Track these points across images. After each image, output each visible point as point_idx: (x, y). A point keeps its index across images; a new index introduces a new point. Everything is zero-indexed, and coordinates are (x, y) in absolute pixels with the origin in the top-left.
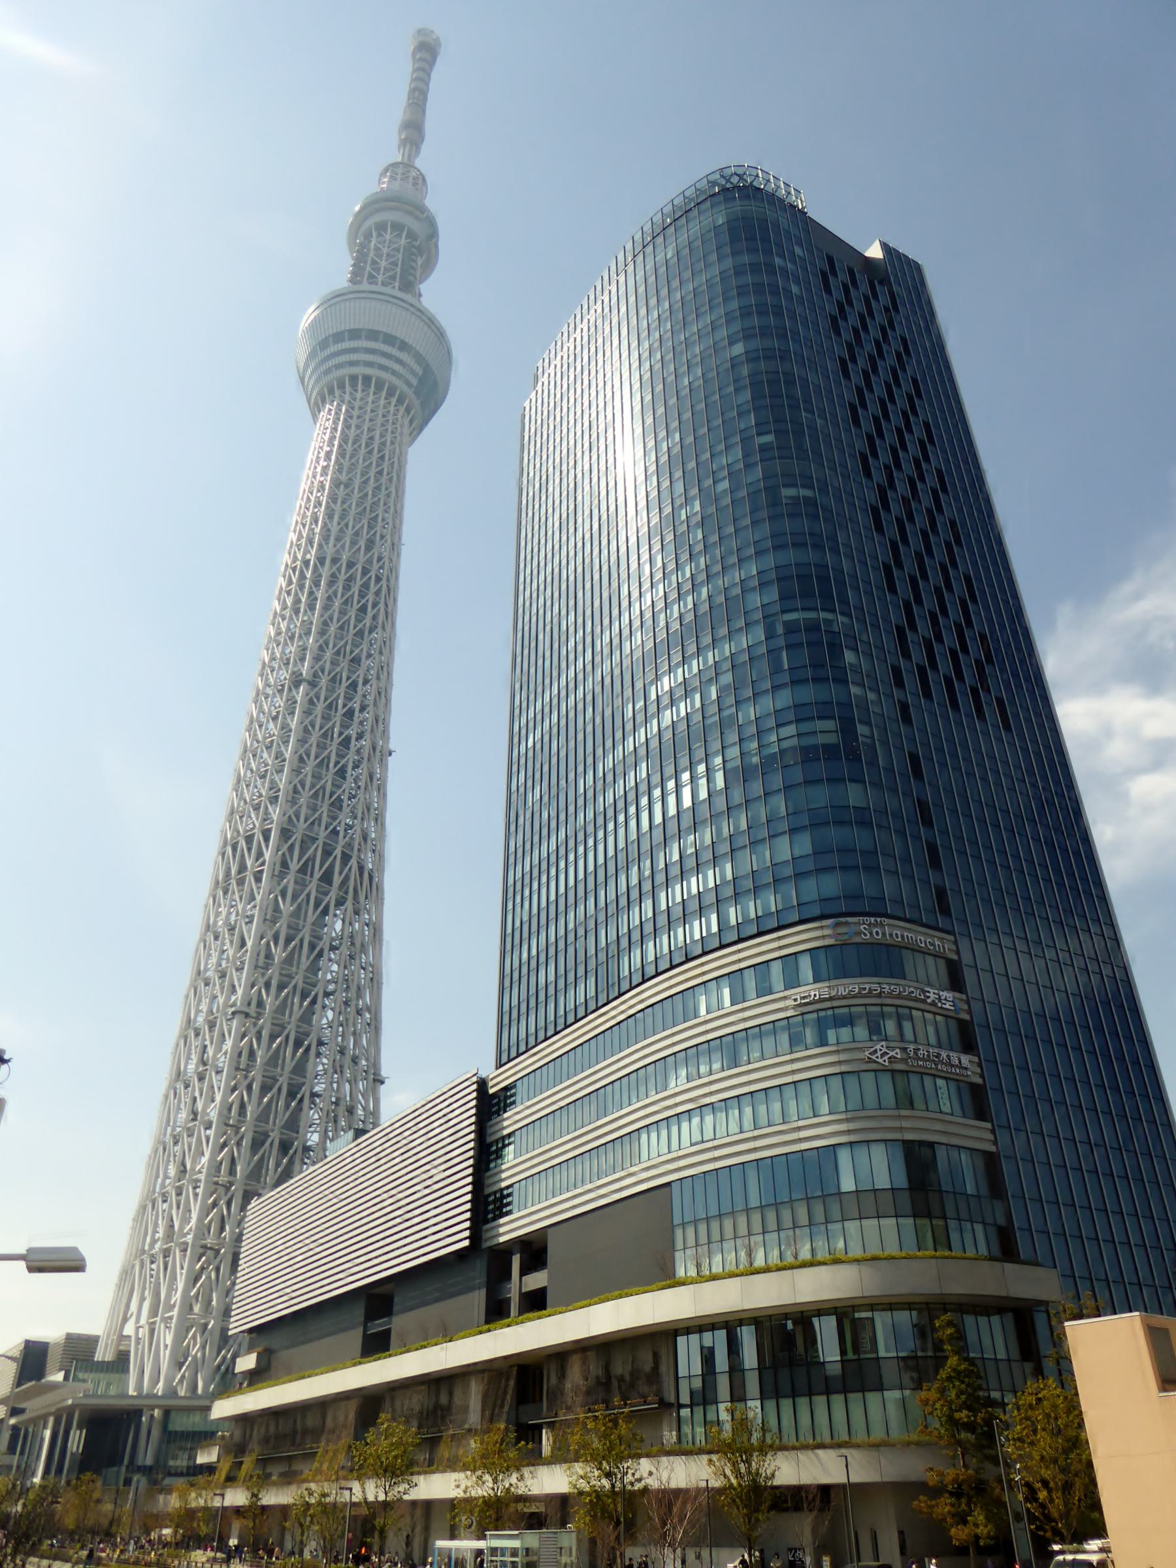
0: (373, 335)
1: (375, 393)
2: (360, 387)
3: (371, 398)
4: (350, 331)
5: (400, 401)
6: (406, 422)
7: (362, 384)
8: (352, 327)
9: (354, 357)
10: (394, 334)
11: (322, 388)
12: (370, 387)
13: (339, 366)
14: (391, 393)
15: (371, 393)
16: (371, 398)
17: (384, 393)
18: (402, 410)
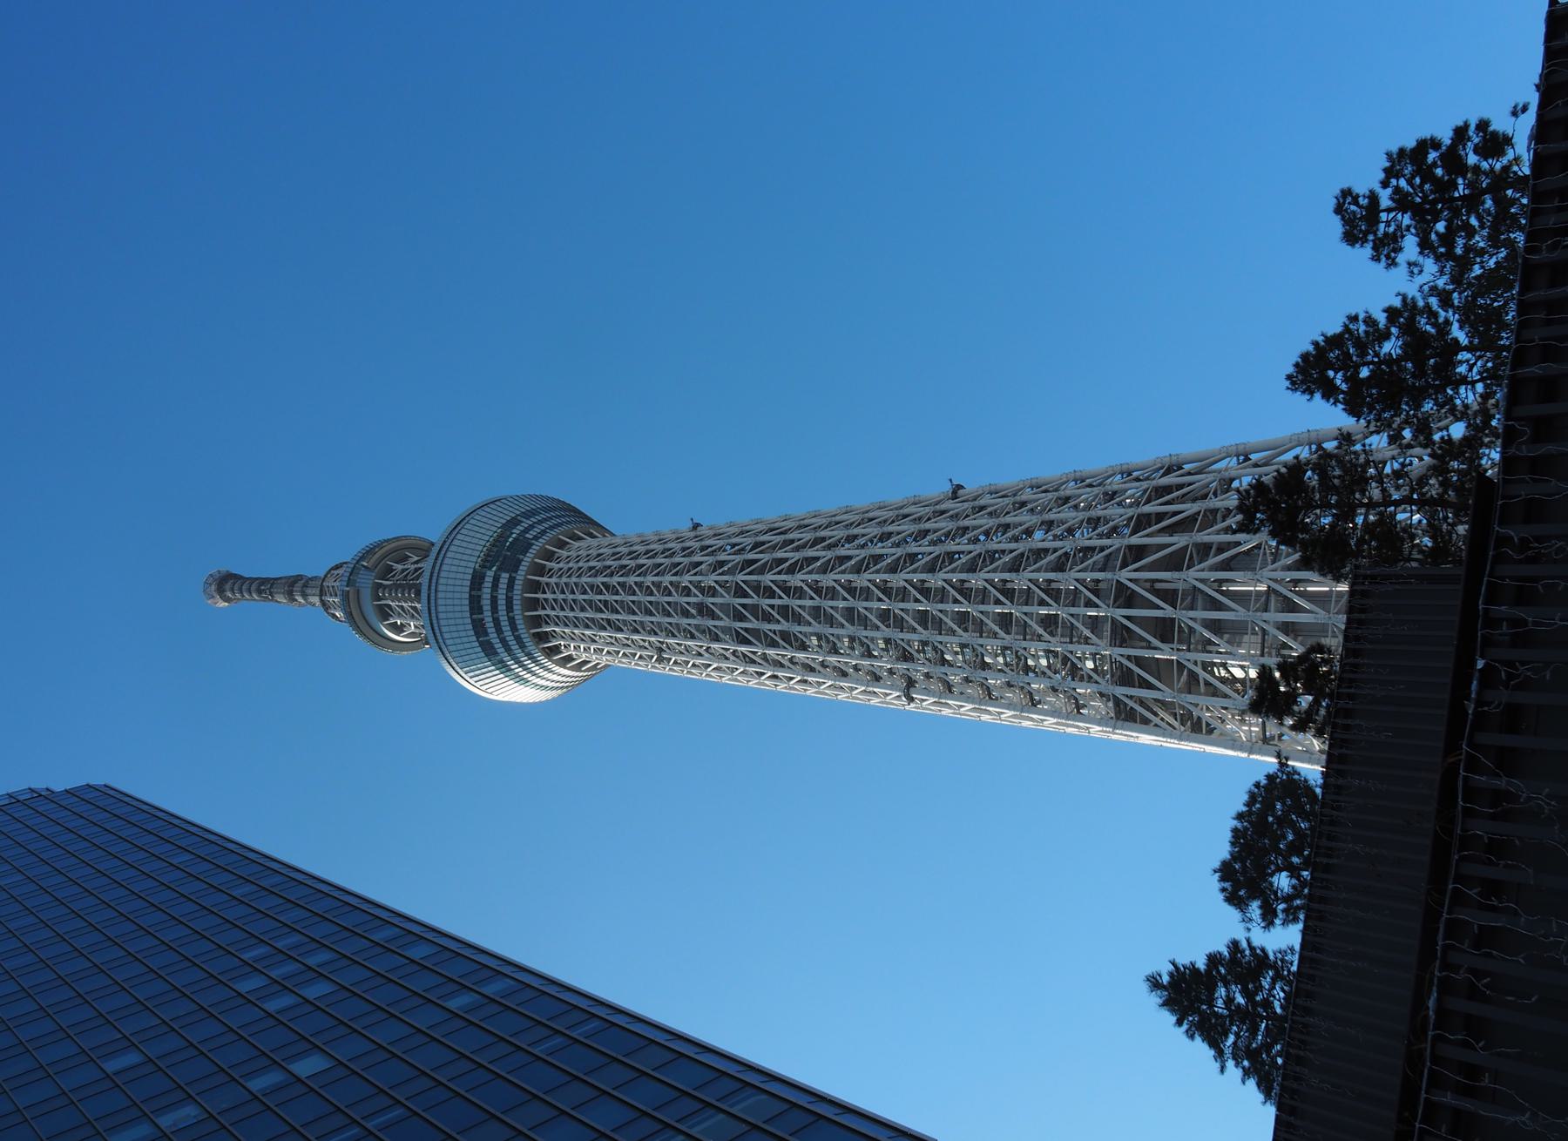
0: (475, 605)
1: (544, 592)
2: (541, 612)
3: (549, 596)
4: (477, 635)
5: (549, 556)
6: (577, 544)
7: (537, 610)
8: (472, 633)
9: (505, 623)
10: (470, 577)
11: (554, 662)
12: (538, 599)
13: (519, 639)
14: (540, 570)
15: (545, 596)
16: (549, 596)
17: (544, 579)
18: (564, 553)
